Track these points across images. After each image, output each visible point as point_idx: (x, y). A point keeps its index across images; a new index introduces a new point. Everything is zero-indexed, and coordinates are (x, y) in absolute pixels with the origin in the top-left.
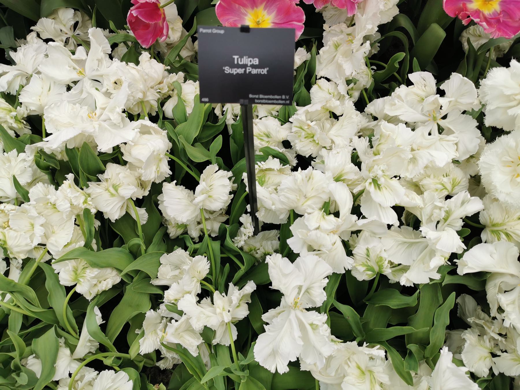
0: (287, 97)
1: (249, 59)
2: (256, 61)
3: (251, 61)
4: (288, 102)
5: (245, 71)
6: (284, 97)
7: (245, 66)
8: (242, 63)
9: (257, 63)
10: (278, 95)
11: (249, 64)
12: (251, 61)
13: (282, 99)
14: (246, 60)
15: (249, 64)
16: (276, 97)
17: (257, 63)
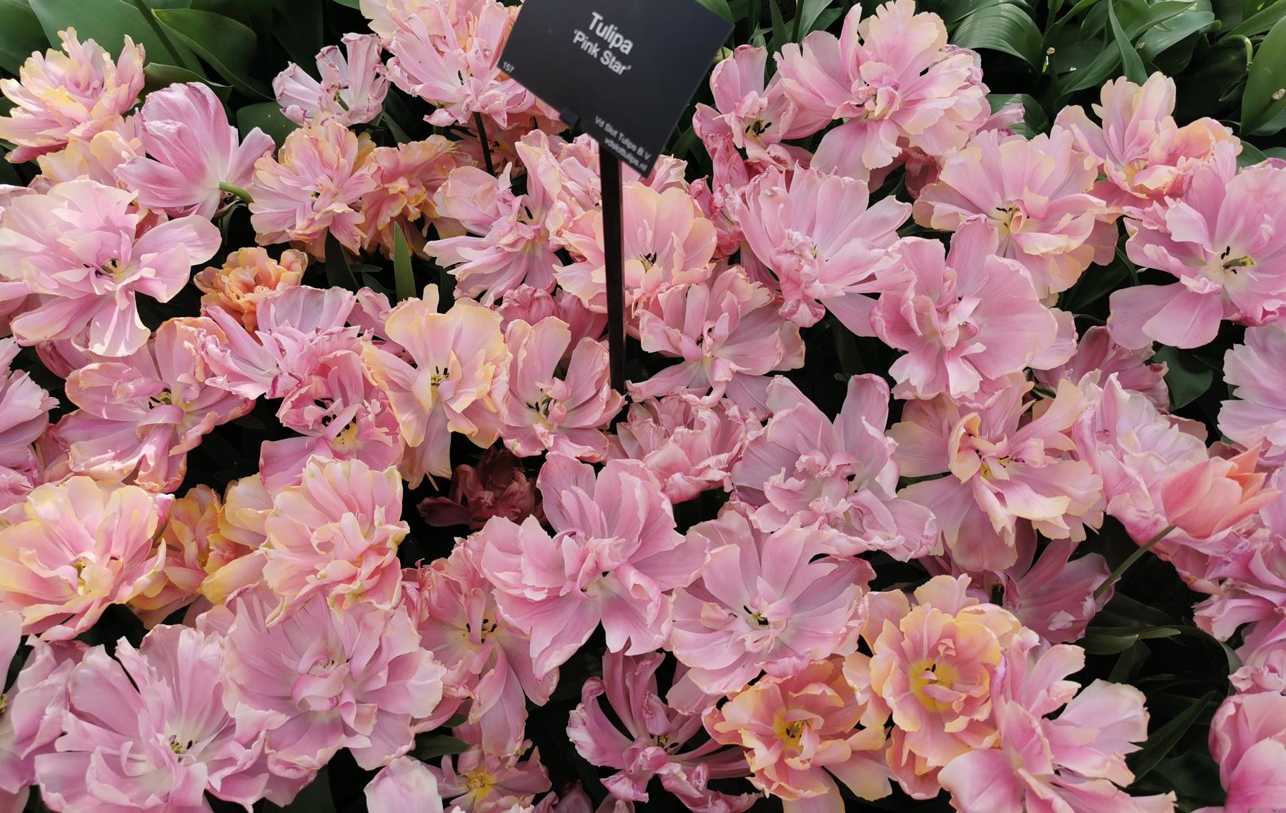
0: (647, 157)
1: (618, 36)
2: (627, 47)
3: (618, 41)
4: (644, 167)
5: (600, 54)
6: (641, 151)
7: (603, 44)
8: (601, 35)
9: (627, 52)
10: (634, 141)
11: (613, 44)
12: (618, 41)
13: (635, 154)
14: (610, 34)
15: (613, 44)
16: (627, 142)
17: (627, 52)
